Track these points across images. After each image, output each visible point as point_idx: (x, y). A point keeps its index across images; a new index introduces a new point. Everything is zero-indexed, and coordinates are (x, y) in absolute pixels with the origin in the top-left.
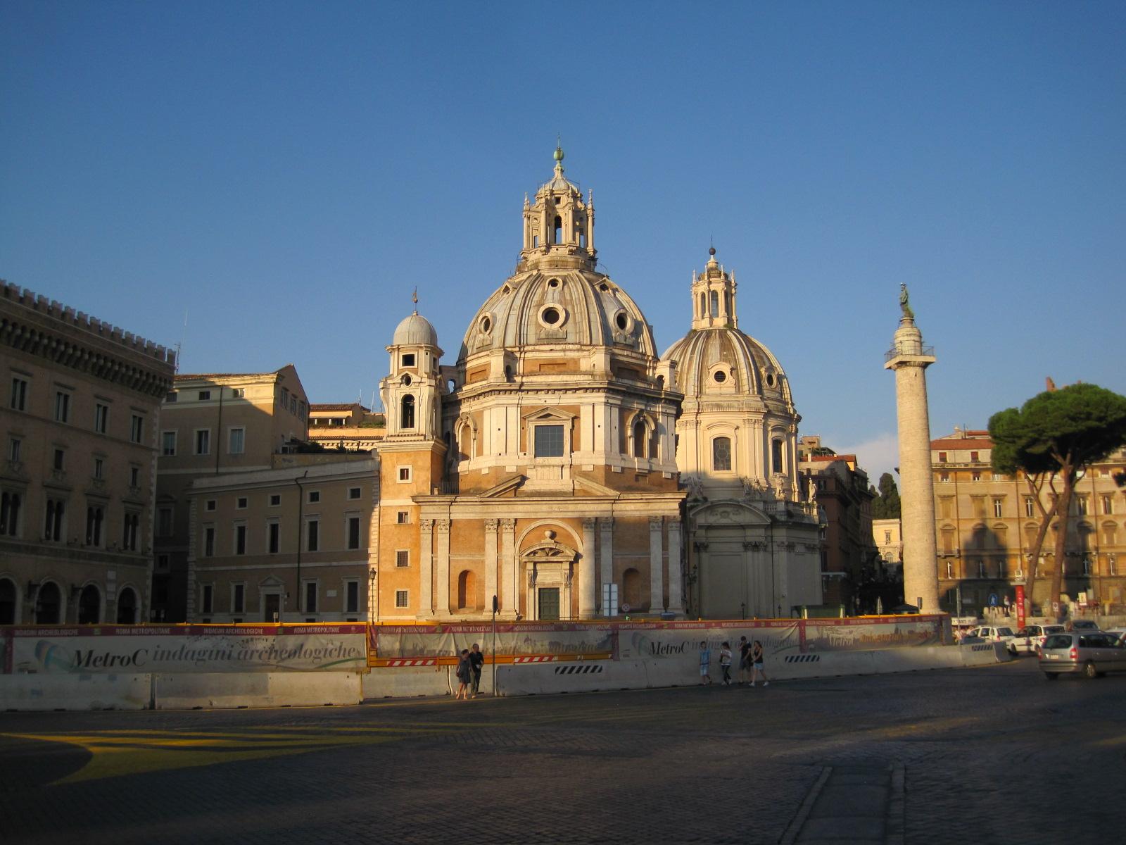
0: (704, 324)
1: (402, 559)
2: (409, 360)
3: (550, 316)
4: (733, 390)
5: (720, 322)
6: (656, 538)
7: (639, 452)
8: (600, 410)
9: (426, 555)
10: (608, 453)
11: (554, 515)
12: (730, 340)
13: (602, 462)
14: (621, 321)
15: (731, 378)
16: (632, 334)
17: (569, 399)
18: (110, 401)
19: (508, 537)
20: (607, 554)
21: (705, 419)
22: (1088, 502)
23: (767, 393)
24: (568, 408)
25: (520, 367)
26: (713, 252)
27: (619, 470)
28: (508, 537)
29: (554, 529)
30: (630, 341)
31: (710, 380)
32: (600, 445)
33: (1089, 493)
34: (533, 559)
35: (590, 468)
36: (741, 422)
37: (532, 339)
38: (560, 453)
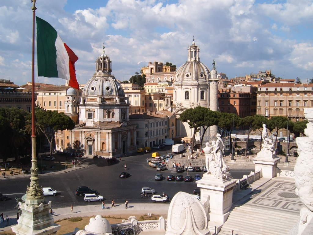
0: (189, 60)
1: (68, 137)
2: (68, 98)
3: (93, 88)
4: (190, 79)
5: (193, 60)
6: (107, 136)
7: (109, 117)
8: (99, 110)
9: (70, 137)
10: (101, 118)
12: (192, 65)
14: (108, 89)
15: (190, 76)
16: (110, 91)
17: (93, 107)
18: (21, 106)
19: (83, 135)
20: (99, 139)
21: (183, 87)
22: (307, 103)
23: (199, 80)
24: (94, 109)
25: (87, 100)
26: (194, 40)
28: (83, 135)
29: (91, 134)
30: (109, 93)
31: (185, 77)
32: (99, 118)
33: (307, 100)
34: (88, 139)
35: (97, 122)
36: (192, 87)
37: (89, 94)
38: (92, 118)
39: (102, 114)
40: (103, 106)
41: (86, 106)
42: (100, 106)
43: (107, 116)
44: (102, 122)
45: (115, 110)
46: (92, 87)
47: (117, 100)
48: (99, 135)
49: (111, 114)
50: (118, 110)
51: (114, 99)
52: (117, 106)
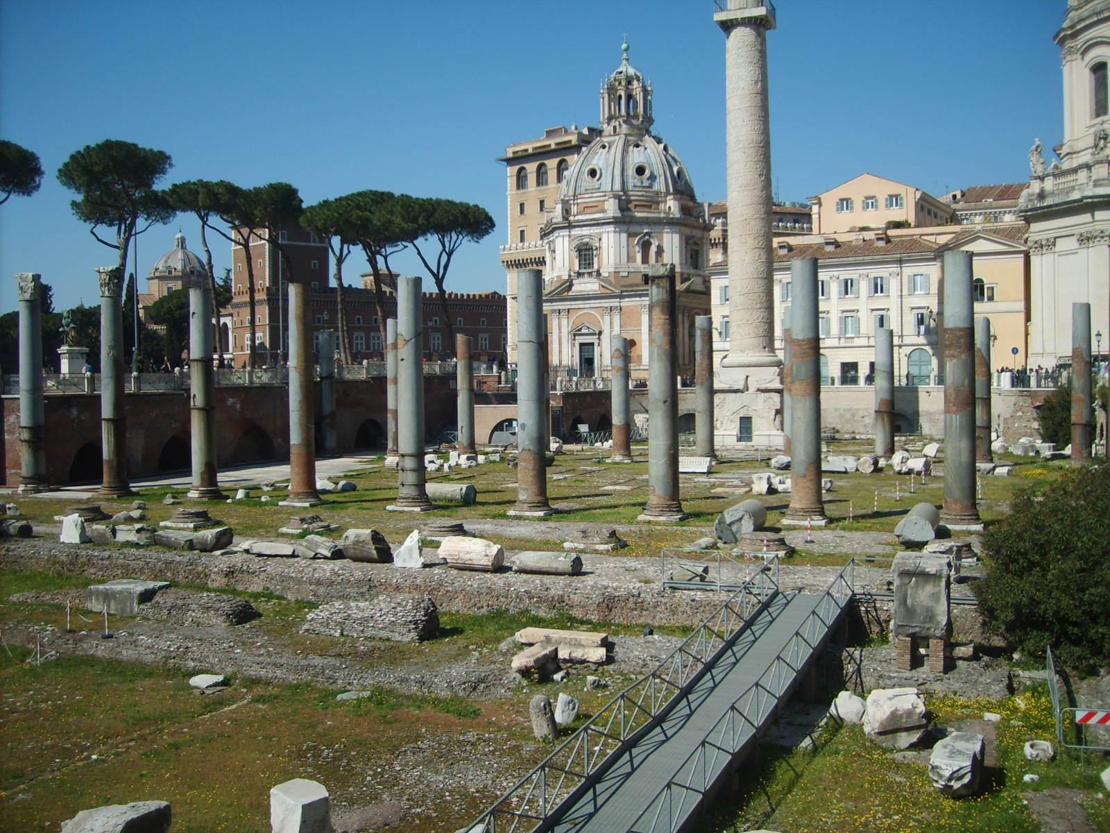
7: (645, 260)
8: (611, 235)
11: (587, 306)
13: (612, 270)
19: (564, 321)
25: (574, 209)
27: (626, 274)
28: (564, 321)
39: (624, 251)
40: (624, 223)
41: (575, 227)
42: (616, 222)
43: (639, 257)
44: (622, 274)
45: (665, 235)
46: (591, 167)
47: (672, 206)
48: (617, 319)
49: (653, 249)
50: (676, 237)
51: (662, 206)
52: (671, 223)
